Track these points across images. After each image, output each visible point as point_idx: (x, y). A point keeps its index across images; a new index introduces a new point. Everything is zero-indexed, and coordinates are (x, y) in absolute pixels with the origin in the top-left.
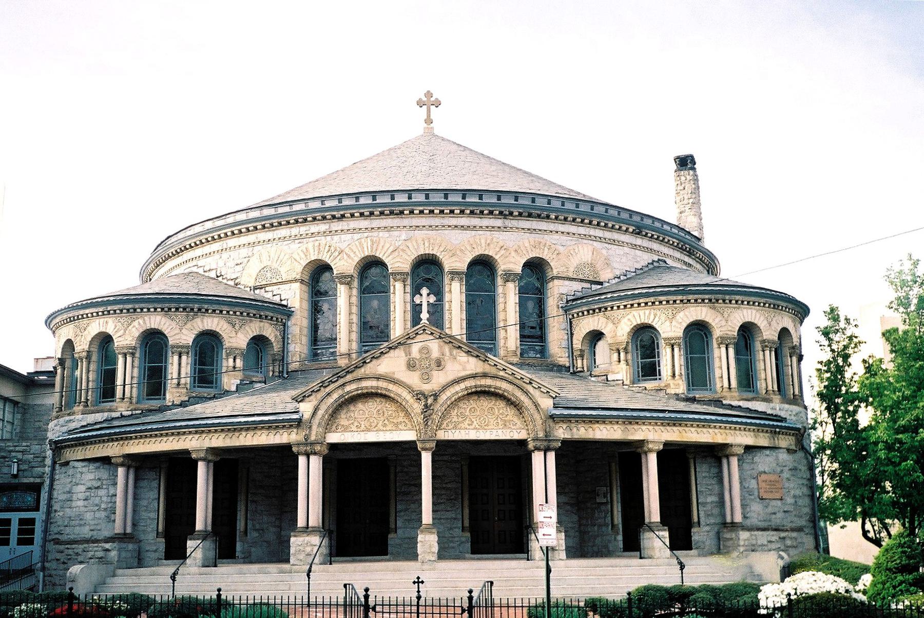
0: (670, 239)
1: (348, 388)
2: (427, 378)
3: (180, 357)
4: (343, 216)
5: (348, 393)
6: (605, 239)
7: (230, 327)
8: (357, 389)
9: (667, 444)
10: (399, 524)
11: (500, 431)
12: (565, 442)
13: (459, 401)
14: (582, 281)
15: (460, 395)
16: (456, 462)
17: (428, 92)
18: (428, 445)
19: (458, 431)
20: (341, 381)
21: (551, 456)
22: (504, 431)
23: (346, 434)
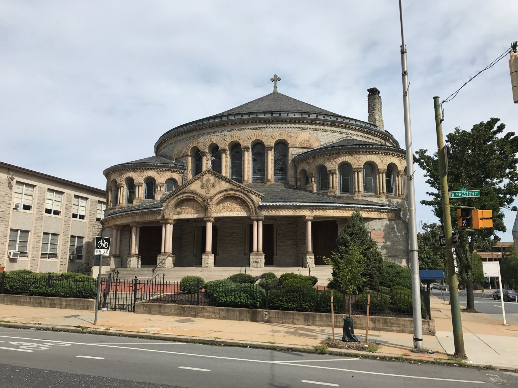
0: (353, 126)
1: (179, 197)
2: (208, 192)
3: (139, 187)
4: (203, 128)
5: (179, 199)
6: (315, 129)
7: (158, 175)
9: (315, 217)
10: (220, 253)
11: (239, 213)
12: (266, 217)
14: (302, 148)
15: (222, 198)
17: (275, 75)
19: (222, 213)
21: (261, 223)
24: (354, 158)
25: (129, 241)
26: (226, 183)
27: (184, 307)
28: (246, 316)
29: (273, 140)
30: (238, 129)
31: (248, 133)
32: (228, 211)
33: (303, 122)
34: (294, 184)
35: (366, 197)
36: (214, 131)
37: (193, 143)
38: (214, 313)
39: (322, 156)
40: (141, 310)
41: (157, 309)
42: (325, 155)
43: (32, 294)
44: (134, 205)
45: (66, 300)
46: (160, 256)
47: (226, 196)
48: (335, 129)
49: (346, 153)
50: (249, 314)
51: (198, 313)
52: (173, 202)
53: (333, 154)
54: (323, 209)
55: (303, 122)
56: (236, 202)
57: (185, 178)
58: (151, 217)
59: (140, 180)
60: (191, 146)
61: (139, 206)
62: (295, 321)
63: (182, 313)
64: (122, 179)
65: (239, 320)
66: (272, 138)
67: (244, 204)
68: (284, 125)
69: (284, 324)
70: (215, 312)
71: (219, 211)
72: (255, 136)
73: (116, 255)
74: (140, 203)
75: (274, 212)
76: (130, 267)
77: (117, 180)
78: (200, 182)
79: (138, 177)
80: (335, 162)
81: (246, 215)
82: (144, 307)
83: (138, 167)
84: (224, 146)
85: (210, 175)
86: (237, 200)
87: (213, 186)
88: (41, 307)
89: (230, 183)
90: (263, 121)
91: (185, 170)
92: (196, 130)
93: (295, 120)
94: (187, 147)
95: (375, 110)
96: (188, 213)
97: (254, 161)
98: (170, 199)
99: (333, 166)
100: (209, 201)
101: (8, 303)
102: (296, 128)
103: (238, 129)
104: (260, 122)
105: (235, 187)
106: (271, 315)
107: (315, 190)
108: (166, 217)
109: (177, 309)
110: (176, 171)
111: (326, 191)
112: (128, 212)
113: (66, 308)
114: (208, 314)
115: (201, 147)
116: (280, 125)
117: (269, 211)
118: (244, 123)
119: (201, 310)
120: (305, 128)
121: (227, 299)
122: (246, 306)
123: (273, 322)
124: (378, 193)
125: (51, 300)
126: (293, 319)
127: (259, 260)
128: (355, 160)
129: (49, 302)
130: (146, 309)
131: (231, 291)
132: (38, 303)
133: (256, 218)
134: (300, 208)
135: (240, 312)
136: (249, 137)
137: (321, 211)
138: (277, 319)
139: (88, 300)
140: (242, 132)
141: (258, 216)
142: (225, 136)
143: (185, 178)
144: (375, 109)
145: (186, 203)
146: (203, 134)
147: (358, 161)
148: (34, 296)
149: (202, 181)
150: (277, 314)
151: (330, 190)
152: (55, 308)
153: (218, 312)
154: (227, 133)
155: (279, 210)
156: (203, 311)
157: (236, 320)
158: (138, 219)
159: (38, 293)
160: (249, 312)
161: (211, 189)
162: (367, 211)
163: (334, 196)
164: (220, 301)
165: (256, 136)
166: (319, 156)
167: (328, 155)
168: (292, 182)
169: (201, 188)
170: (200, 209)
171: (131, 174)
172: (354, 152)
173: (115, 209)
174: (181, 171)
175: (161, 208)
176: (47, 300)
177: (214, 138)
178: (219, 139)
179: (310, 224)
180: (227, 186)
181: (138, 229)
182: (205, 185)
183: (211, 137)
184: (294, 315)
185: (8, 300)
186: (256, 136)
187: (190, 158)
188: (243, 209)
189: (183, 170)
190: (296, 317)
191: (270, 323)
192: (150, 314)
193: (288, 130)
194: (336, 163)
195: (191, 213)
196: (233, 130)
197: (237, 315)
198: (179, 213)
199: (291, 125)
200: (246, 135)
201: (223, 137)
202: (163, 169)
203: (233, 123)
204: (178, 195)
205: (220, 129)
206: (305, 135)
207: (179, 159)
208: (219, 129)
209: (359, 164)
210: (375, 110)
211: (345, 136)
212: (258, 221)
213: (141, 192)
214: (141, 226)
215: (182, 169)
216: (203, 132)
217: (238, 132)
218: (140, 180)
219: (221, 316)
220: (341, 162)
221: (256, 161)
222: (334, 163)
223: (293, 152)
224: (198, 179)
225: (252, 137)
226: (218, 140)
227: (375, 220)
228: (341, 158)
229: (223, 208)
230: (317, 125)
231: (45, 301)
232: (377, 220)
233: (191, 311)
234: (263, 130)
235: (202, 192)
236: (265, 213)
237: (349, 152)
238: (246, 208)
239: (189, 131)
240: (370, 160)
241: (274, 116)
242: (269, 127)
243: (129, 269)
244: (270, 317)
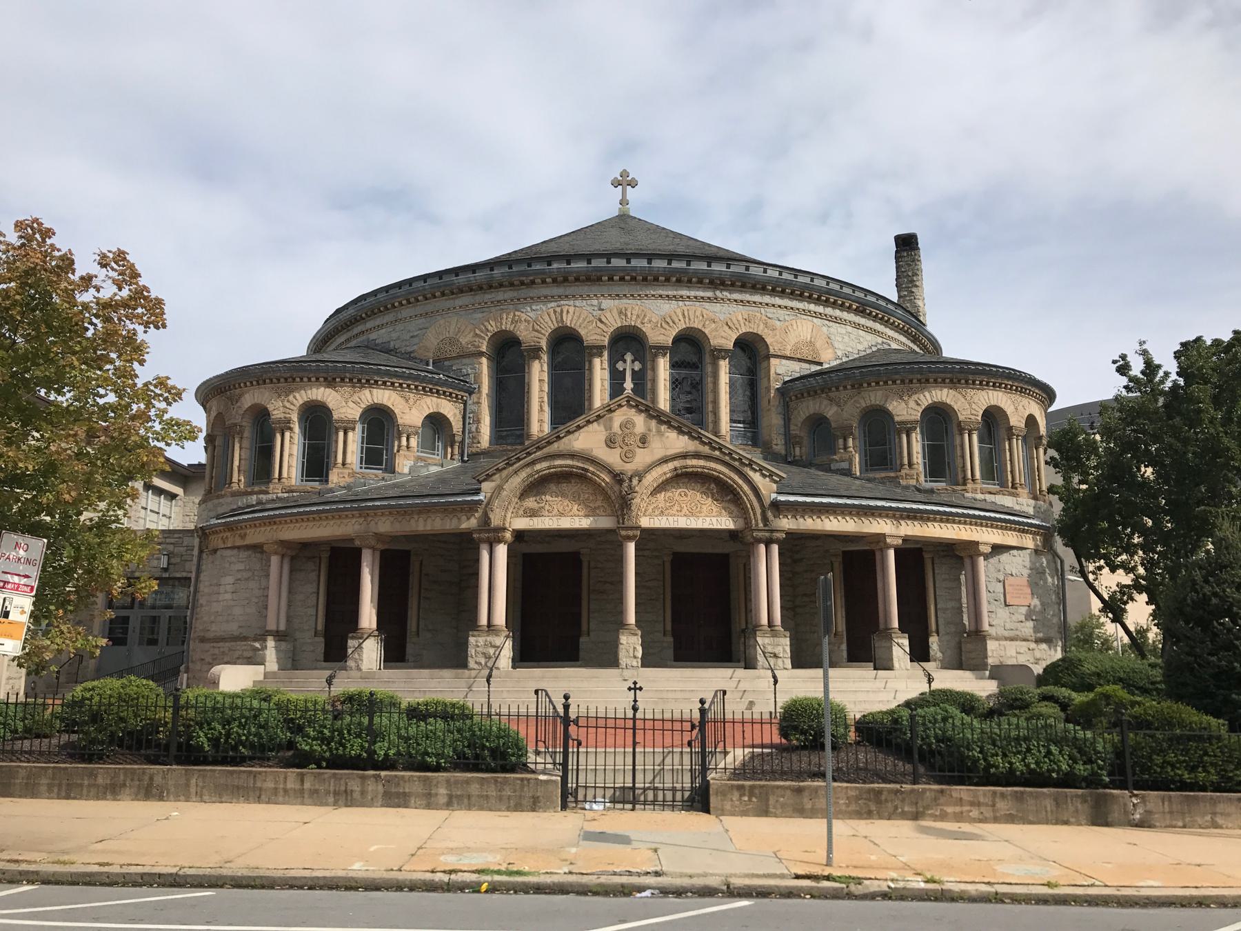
0: (896, 320)
1: (538, 467)
2: (627, 457)
3: (345, 434)
4: (533, 282)
5: (538, 472)
6: (826, 315)
7: (402, 401)
8: (549, 468)
9: (906, 539)
10: (592, 626)
11: (714, 520)
12: (791, 534)
13: (667, 484)
14: (800, 360)
15: (668, 476)
16: (657, 557)
17: (625, 170)
18: (630, 533)
19: (665, 518)
20: (529, 459)
21: (775, 548)
22: (719, 519)
23: (535, 519)
24: (960, 396)
25: (315, 590)
26: (681, 437)
27: (880, 792)
28: (1077, 811)
29: (730, 332)
30: (639, 295)
31: (666, 307)
32: (683, 513)
33: (801, 295)
34: (783, 452)
35: (990, 493)
36: (567, 293)
37: (499, 320)
38: (975, 804)
39: (881, 383)
40: (732, 806)
41: (788, 798)
42: (890, 382)
43: (301, 760)
44: (331, 485)
45: (448, 781)
46: (479, 636)
47: (680, 472)
48: (863, 321)
49: (943, 381)
50: (1086, 806)
51: (927, 807)
52: (517, 481)
53: (911, 381)
54: (922, 519)
55: (801, 295)
56: (704, 489)
57: (471, 415)
58: (438, 520)
59: (352, 412)
60: (489, 327)
61: (348, 487)
62: (1220, 820)
63: (873, 808)
64: (288, 405)
65: (1056, 824)
66: (730, 328)
67: (727, 495)
68: (757, 298)
69: (1189, 828)
70: (979, 802)
71: (657, 513)
72: (684, 317)
73: (277, 631)
74: (352, 480)
75: (809, 521)
76: (359, 669)
77: (270, 407)
78: (602, 428)
79: (344, 404)
80: (916, 401)
81: (732, 526)
82: (741, 796)
83: (348, 375)
84: (598, 337)
85: (633, 410)
86: (707, 485)
87: (644, 443)
88: (347, 806)
89: (692, 438)
90: (708, 281)
91: (471, 393)
92: (512, 284)
93: (784, 287)
94: (478, 332)
95: (916, 286)
96: (561, 514)
97: (673, 383)
98: (505, 473)
99: (911, 411)
100: (635, 481)
101: (206, 798)
102: (786, 307)
103: (639, 295)
104: (700, 282)
105: (706, 450)
106: (1150, 806)
107: (857, 470)
108: (495, 521)
109: (858, 798)
110: (451, 394)
111: (892, 474)
112: (357, 504)
113: (449, 805)
114: (958, 809)
115: (525, 333)
116: (747, 297)
117: (806, 517)
118: (611, 279)
119: (936, 799)
120: (804, 310)
121: (1011, 763)
122: (1068, 781)
123: (1158, 824)
124: (1010, 485)
125: (388, 780)
126: (1214, 814)
127: (780, 648)
128: (963, 400)
129: (380, 788)
130: (750, 800)
131: (1017, 739)
132: (336, 793)
133: (767, 534)
134: (873, 515)
135: (1056, 800)
136: (668, 320)
137: (916, 523)
138: (1168, 816)
139: (537, 779)
140: (650, 304)
141: (772, 531)
142: (601, 309)
143: (471, 415)
144: (917, 283)
145: (553, 487)
146: (532, 298)
147: (969, 404)
148: (312, 770)
149: (608, 427)
150: (1166, 803)
151: (903, 472)
152: (407, 807)
153: (988, 800)
154: (607, 303)
155: (823, 517)
156: (942, 800)
157: (1047, 822)
158: (385, 526)
159: (327, 760)
160: (1083, 797)
161: (638, 450)
162: (1001, 528)
163: (915, 487)
164: (993, 770)
165: (687, 319)
166: (873, 384)
167: (898, 382)
168: (779, 447)
169: (608, 446)
170: (599, 503)
171: (321, 394)
172: (963, 381)
173: (267, 493)
174: (462, 397)
175: (476, 498)
176: (374, 781)
177: (568, 312)
178: (583, 316)
179: (891, 554)
180: (683, 445)
181: (378, 554)
182: (619, 439)
183: (558, 309)
184: (1214, 802)
185: (203, 787)
186: (687, 319)
187: (484, 360)
188: (724, 508)
189: (467, 394)
190: (1220, 807)
191: (1149, 827)
192: (767, 816)
193: (768, 310)
194: (918, 404)
195: (571, 513)
196: (625, 295)
197: (1049, 809)
198: (533, 513)
199: (773, 299)
200: (662, 313)
201: (595, 313)
202: (416, 387)
203: (627, 278)
204: (533, 463)
205: (586, 288)
206: (805, 328)
207: (447, 363)
208: (584, 289)
209: (973, 412)
210: (916, 286)
211: (880, 340)
212: (768, 543)
213: (351, 447)
214: (386, 547)
215: (462, 389)
216: (533, 292)
217: (639, 302)
218: (349, 411)
219: (998, 815)
220: (930, 402)
221: (680, 383)
222: (912, 404)
223: (781, 370)
224: (596, 421)
225: (676, 321)
226: (579, 317)
227: (1011, 552)
228: (930, 392)
229: (668, 504)
230: (828, 307)
231: (363, 784)
232: (1015, 552)
233: (903, 800)
234: (707, 305)
235: (612, 458)
236: (787, 523)
237: (951, 381)
238: (732, 507)
239: (484, 287)
240: (995, 403)
241: (733, 269)
242: (723, 299)
243: (354, 673)
244: (1149, 812)
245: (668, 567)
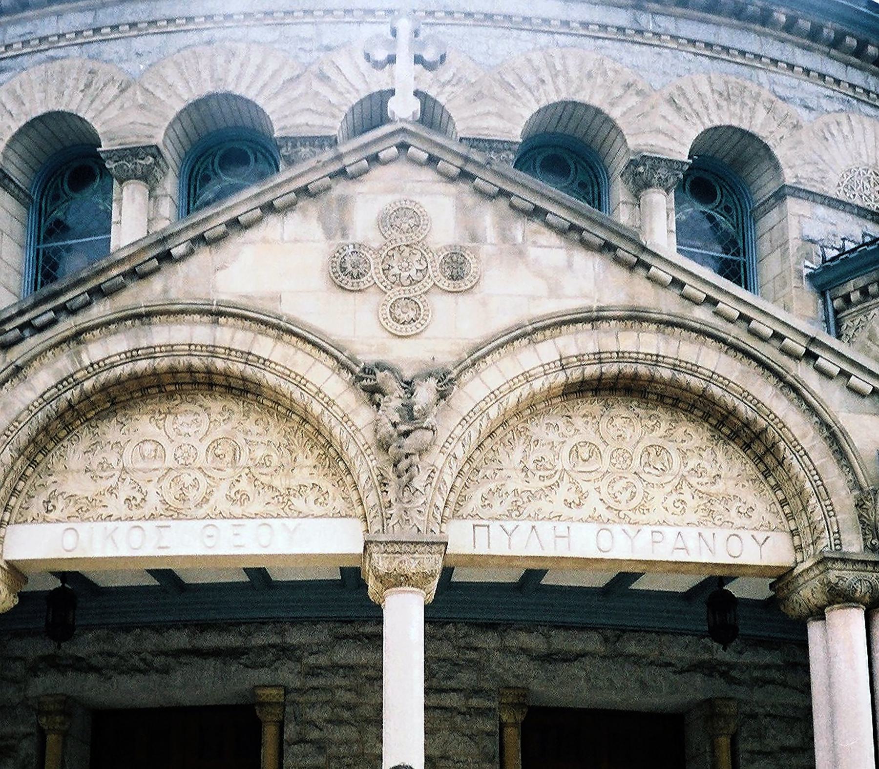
5: (95, 368)
8: (132, 356)
13: (534, 414)
15: (537, 385)
16: (482, 712)
18: (411, 565)
20: (67, 326)
22: (707, 533)
23: (84, 528)
29: (679, 121)
100: (425, 394)
136: (510, 79)
245: (513, 737)
